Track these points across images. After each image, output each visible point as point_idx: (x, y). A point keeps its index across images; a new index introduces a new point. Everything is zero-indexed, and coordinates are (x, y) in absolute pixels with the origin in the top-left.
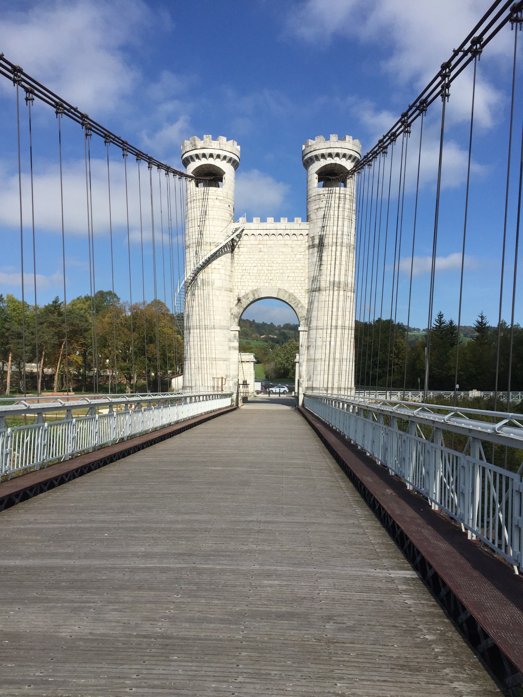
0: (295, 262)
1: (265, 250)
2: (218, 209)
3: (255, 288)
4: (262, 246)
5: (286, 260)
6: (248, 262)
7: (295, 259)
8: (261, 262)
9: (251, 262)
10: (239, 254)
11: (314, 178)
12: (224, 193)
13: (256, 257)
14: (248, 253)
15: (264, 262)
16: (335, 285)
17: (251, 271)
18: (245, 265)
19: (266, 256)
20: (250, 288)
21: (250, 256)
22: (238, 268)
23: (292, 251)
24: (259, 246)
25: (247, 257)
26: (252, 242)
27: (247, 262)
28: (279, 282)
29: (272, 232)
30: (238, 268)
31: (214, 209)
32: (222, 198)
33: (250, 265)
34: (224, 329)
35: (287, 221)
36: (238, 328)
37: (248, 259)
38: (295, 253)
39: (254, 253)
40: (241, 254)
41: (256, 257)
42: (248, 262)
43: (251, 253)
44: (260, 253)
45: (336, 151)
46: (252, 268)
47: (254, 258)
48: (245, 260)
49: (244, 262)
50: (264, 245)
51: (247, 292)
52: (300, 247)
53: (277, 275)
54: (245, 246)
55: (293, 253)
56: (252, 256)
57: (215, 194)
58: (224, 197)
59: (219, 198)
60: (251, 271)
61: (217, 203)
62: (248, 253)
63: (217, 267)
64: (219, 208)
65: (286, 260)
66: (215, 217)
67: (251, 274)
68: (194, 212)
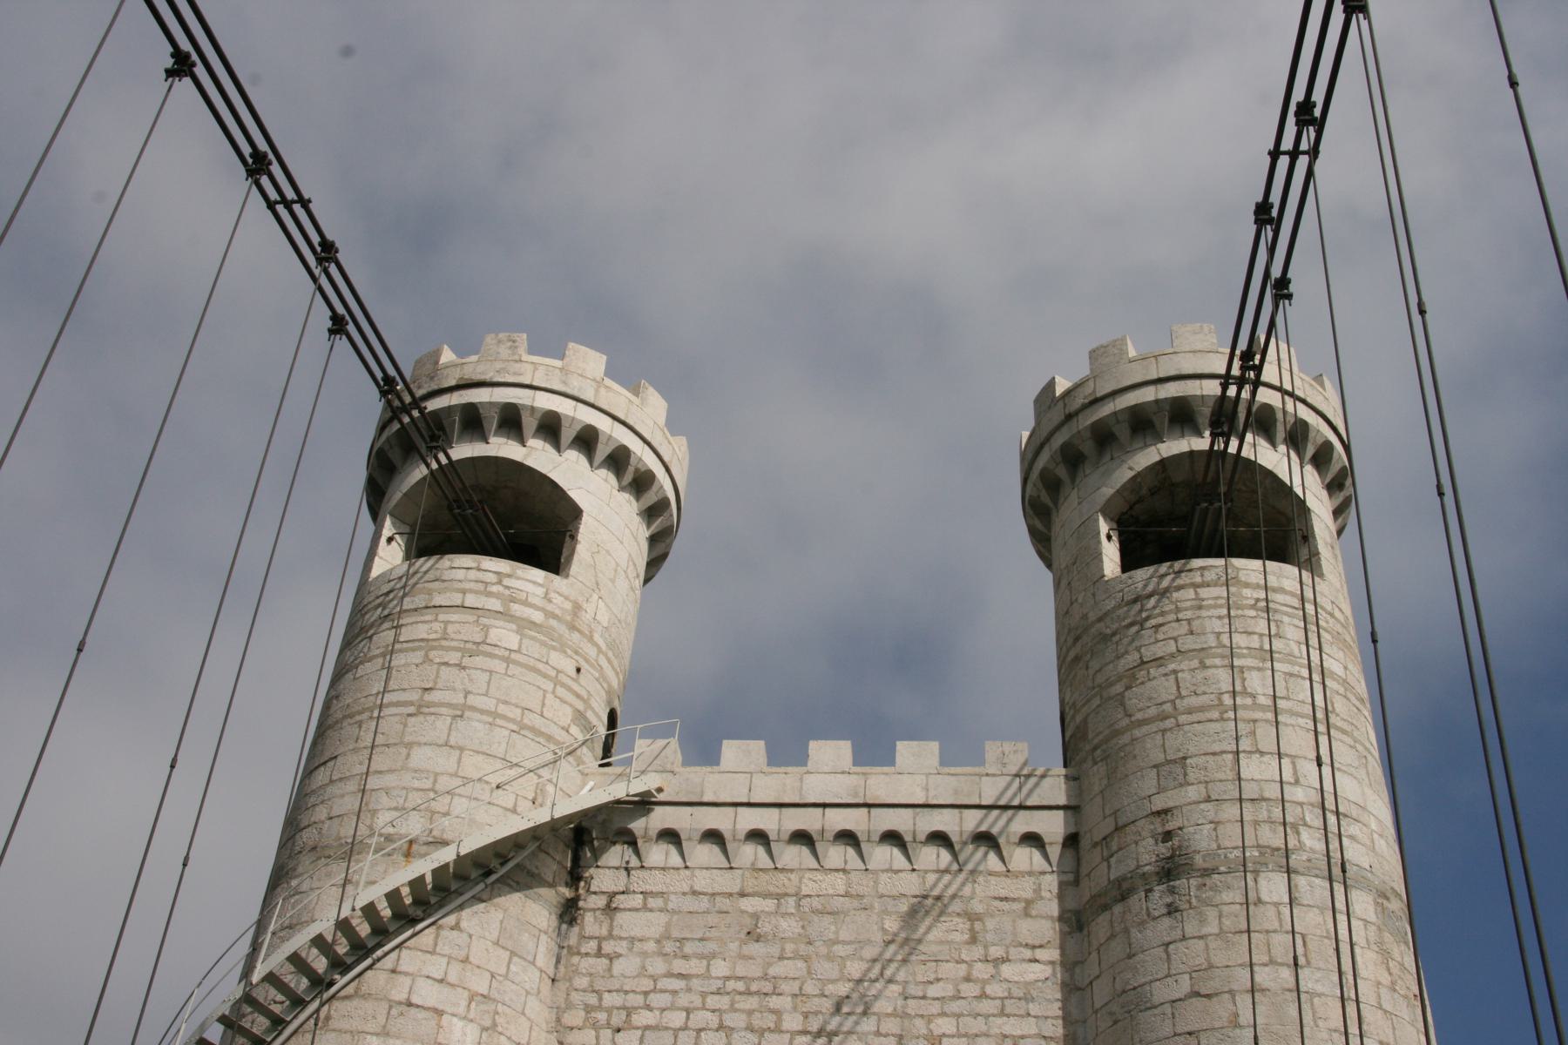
0: (987, 1006)
1: (789, 926)
2: (499, 666)
4: (769, 905)
5: (933, 991)
6: (664, 1000)
7: (994, 989)
8: (752, 1003)
9: (683, 1000)
10: (608, 947)
12: (557, 599)
13: (720, 968)
14: (669, 947)
15: (774, 1002)
19: (795, 968)
21: (679, 966)
23: (973, 940)
24: (749, 904)
25: (657, 966)
26: (702, 881)
27: (657, 1000)
31: (478, 661)
32: (538, 617)
33: (677, 1019)
35: (934, 761)
37: (665, 983)
38: (996, 952)
39: (711, 946)
40: (622, 947)
41: (720, 968)
42: (664, 1000)
43: (689, 948)
44: (754, 948)
47: (707, 976)
48: (647, 984)
49: (638, 1000)
50: (779, 897)
52: (1027, 915)
54: (652, 903)
55: (977, 952)
56: (695, 966)
57: (494, 589)
58: (550, 615)
59: (516, 609)
61: (504, 635)
62: (669, 947)
63: (427, 994)
64: (507, 660)
65: (933, 991)
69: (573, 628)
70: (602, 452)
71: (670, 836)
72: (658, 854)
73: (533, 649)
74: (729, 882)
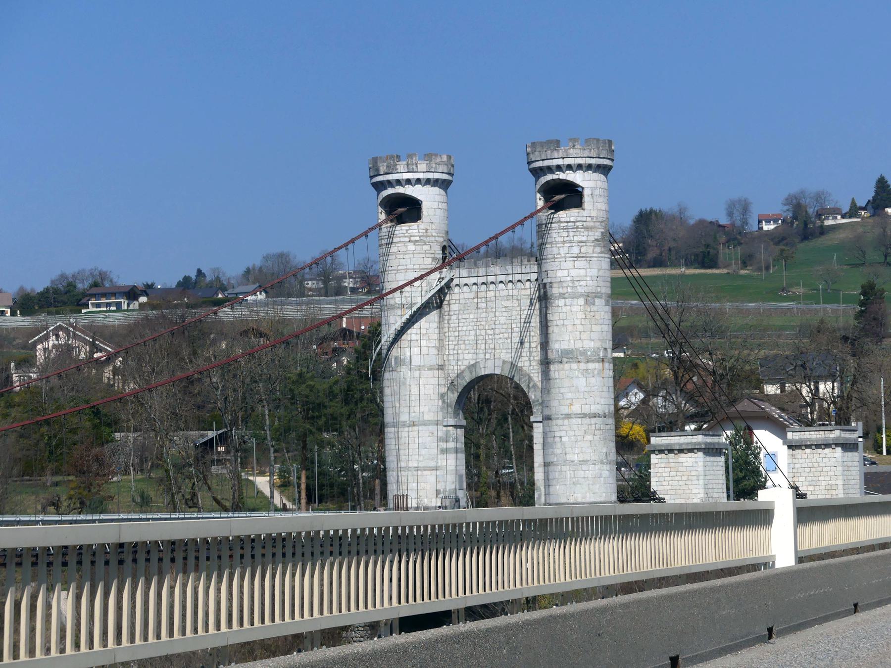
2: (411, 256)
3: (472, 362)
12: (421, 231)
13: (472, 316)
17: (466, 338)
20: (466, 363)
21: (464, 316)
24: (475, 300)
26: (467, 295)
28: (504, 351)
31: (407, 256)
32: (418, 238)
34: (429, 425)
41: (472, 316)
45: (555, 162)
46: (467, 333)
51: (463, 368)
53: (500, 341)
56: (467, 316)
59: (413, 239)
60: (466, 338)
61: (411, 247)
66: (408, 267)
67: (467, 342)
69: (427, 236)
70: (423, 182)
71: (457, 285)
72: (456, 290)
73: (418, 247)
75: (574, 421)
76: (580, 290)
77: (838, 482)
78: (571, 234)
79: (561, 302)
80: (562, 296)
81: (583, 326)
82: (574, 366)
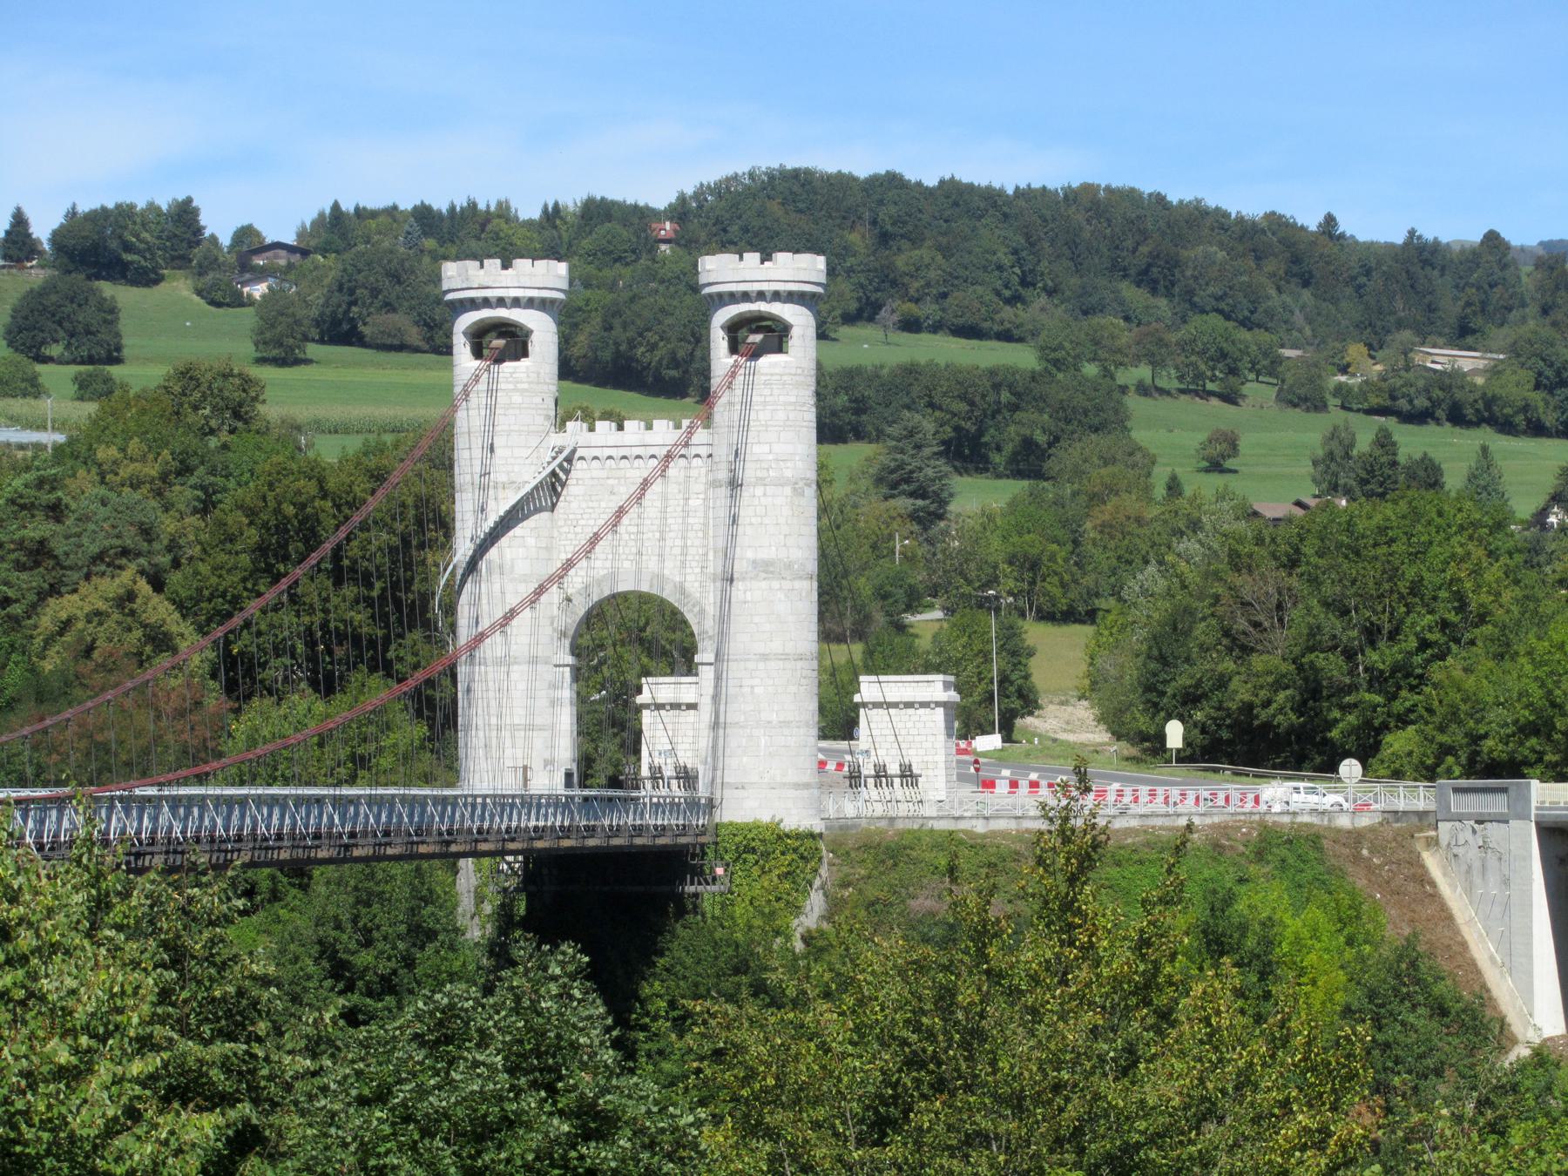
11: (719, 342)
13: (603, 505)
16: (766, 568)
18: (582, 522)
22: (565, 529)
24: (610, 482)
25: (584, 505)
26: (595, 474)
29: (637, 451)
30: (565, 529)
32: (525, 386)
36: (570, 660)
45: (757, 287)
56: (595, 504)
61: (517, 398)
68: (469, 420)
74: (604, 474)
75: (772, 664)
76: (788, 473)
77: (936, 758)
78: (776, 392)
79: (759, 491)
80: (761, 481)
81: (781, 529)
82: (776, 584)
